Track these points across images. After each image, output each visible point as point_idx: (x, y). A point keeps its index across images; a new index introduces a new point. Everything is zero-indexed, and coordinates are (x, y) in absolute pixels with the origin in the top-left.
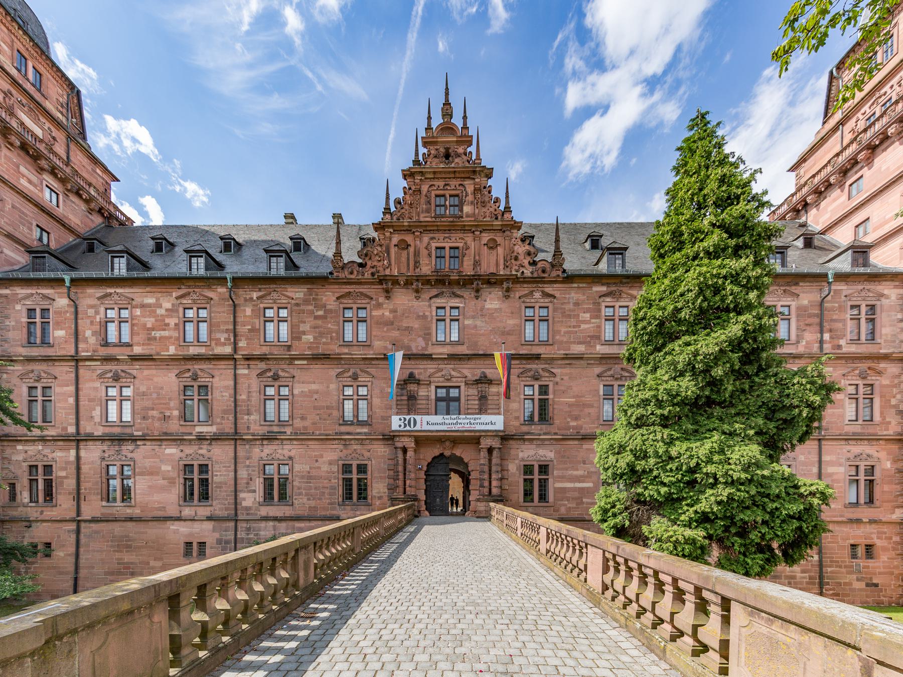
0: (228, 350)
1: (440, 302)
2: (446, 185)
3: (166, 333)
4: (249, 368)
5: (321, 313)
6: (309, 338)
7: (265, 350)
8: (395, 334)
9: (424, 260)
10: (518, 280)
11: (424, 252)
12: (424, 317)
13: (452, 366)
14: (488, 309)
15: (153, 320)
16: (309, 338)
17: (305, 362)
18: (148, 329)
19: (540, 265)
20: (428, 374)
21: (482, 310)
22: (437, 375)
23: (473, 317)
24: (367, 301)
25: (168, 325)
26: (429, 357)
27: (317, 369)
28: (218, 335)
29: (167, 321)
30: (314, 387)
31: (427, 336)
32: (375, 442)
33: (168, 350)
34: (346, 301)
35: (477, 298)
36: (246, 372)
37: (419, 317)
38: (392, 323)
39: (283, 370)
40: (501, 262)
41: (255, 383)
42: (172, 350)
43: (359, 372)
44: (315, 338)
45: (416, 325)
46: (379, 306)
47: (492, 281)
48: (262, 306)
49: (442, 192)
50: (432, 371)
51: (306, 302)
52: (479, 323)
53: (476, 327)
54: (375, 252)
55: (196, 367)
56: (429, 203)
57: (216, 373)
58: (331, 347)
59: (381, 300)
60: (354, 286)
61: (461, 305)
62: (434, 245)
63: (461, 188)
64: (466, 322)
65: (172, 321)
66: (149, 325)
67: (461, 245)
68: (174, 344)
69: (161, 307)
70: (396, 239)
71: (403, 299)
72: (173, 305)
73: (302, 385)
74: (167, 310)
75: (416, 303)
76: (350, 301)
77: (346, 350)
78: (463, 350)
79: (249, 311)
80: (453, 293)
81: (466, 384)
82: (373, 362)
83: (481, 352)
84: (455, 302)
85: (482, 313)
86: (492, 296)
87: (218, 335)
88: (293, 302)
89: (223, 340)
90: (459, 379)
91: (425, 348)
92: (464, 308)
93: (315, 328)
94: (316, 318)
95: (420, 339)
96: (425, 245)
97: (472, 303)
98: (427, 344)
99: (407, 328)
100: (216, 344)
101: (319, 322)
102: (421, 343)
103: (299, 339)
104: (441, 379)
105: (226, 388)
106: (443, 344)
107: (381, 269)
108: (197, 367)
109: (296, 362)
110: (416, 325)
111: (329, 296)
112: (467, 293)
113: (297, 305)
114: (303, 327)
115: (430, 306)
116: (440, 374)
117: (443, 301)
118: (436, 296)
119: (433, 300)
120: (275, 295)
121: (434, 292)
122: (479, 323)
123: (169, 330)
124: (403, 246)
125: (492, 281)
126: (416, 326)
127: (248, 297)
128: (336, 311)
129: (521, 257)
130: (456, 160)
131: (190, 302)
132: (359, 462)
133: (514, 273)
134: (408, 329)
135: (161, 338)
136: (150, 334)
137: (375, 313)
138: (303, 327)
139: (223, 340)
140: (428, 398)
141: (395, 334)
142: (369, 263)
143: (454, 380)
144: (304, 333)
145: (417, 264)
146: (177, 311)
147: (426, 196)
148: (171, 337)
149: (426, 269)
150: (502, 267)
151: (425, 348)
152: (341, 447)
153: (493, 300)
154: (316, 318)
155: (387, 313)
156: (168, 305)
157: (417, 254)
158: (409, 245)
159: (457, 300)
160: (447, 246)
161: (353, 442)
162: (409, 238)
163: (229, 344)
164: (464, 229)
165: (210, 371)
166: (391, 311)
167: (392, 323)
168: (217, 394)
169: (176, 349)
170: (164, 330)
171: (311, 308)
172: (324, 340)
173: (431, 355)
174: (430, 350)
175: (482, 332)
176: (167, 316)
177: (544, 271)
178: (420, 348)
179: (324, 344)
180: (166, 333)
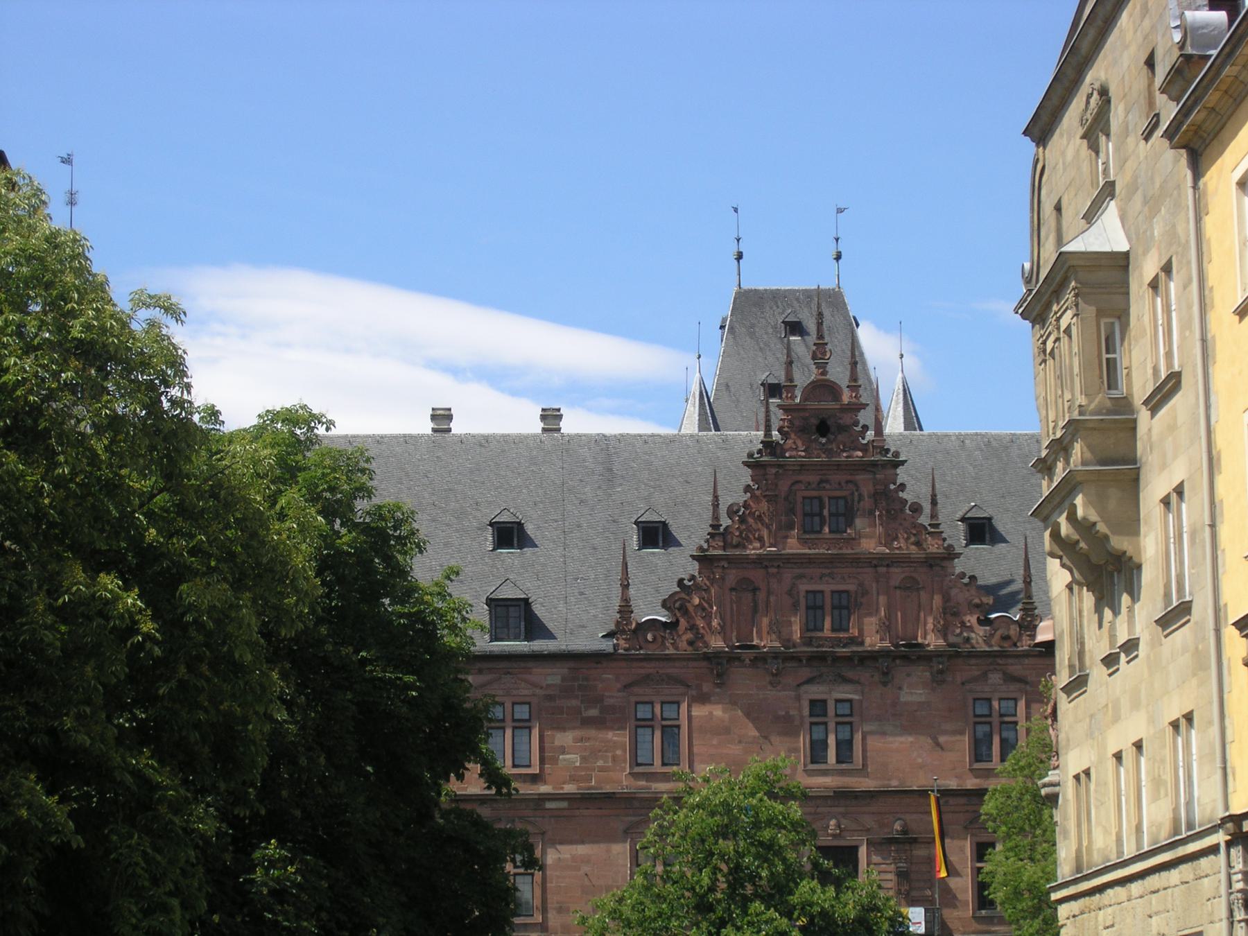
1: (816, 691)
2: (821, 481)
5: (593, 712)
6: (574, 758)
13: (842, 809)
16: (574, 758)
17: (564, 804)
44: (583, 759)
49: (815, 493)
54: (696, 601)
56: (792, 511)
59: (706, 687)
61: (856, 697)
62: (804, 587)
63: (850, 486)
81: (870, 843)
83: (894, 784)
92: (861, 701)
103: (555, 760)
109: (549, 805)
113: (550, 698)
117: (822, 688)
118: (810, 681)
121: (805, 673)
130: (840, 437)
144: (563, 750)
147: (786, 499)
158: (755, 590)
159: (849, 687)
172: (600, 763)
179: (602, 769)
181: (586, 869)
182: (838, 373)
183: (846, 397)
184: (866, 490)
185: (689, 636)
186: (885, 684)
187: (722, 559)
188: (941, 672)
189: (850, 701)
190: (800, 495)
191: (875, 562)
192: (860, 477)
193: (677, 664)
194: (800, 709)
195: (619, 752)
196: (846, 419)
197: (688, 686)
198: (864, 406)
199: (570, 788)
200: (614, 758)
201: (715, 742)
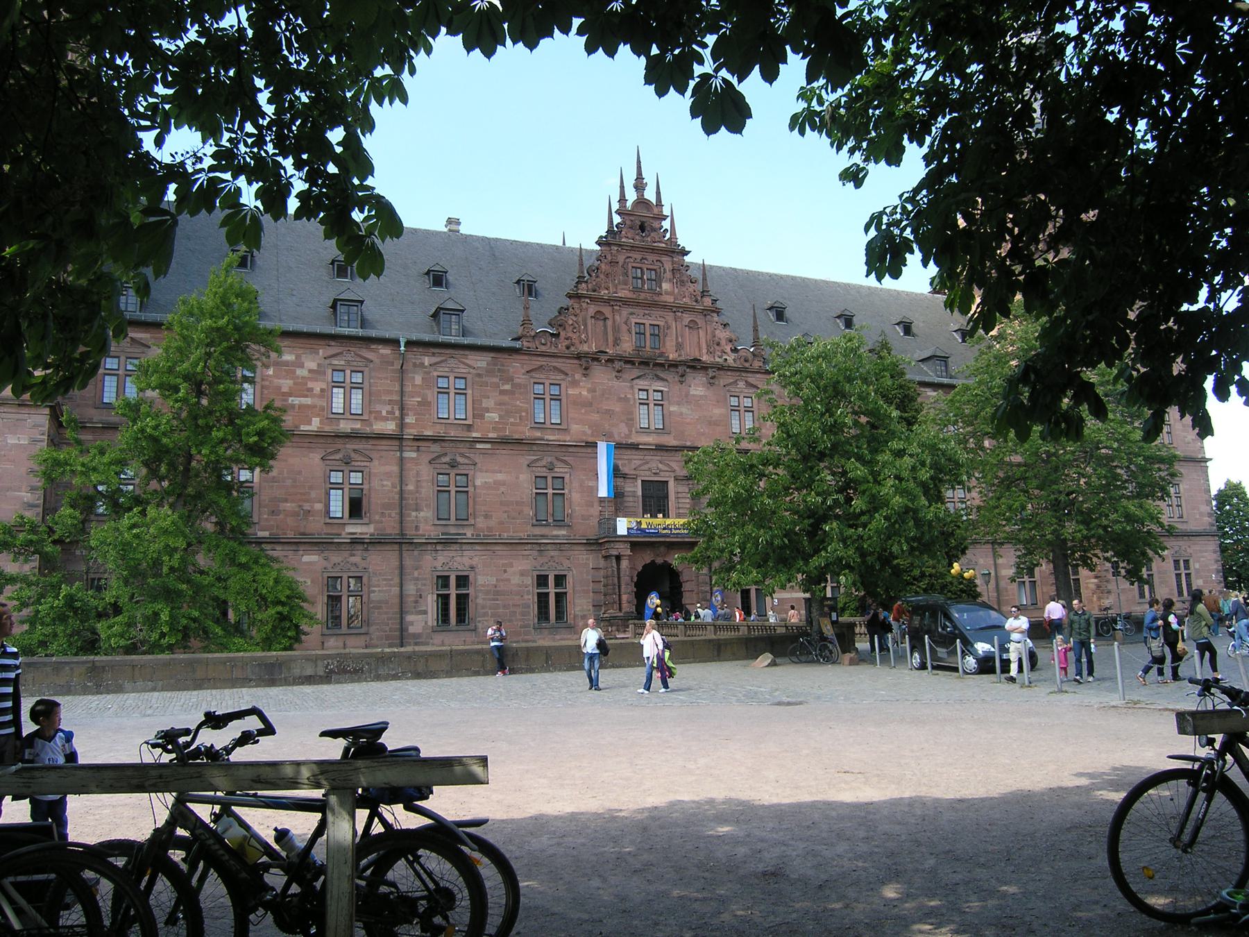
0: (390, 427)
1: (642, 383)
2: (643, 259)
3: (308, 401)
4: (418, 450)
5: (507, 387)
6: (494, 416)
7: (440, 431)
8: (595, 417)
9: (625, 337)
10: (721, 368)
11: (624, 328)
12: (626, 400)
14: (694, 395)
15: (290, 382)
16: (494, 416)
17: (488, 446)
18: (284, 394)
19: (741, 353)
20: (633, 467)
21: (687, 395)
22: (642, 468)
23: (679, 404)
24: (563, 377)
25: (311, 390)
26: (634, 447)
27: (504, 453)
28: (378, 407)
29: (310, 385)
30: (500, 477)
31: (630, 420)
32: (576, 547)
33: (310, 423)
34: (537, 376)
35: (681, 382)
36: (414, 455)
37: (620, 399)
38: (591, 404)
39: (462, 455)
40: (704, 346)
41: (426, 472)
42: (315, 425)
43: (556, 462)
44: (501, 417)
45: (617, 408)
46: (575, 384)
47: (695, 365)
48: (436, 374)
49: (639, 265)
50: (638, 462)
51: (490, 372)
52: (684, 410)
53: (681, 414)
55: (348, 446)
57: (374, 455)
58: (521, 428)
59: (577, 376)
60: (545, 359)
62: (634, 320)
63: (659, 263)
64: (672, 409)
65: (317, 387)
66: (285, 389)
67: (661, 324)
68: (318, 415)
69: (302, 366)
70: (592, 309)
71: (602, 376)
72: (319, 365)
73: (484, 474)
74: (310, 371)
75: (616, 383)
76: (542, 376)
77: (538, 434)
78: (671, 441)
79: (418, 380)
80: (657, 376)
81: (676, 479)
82: (571, 449)
84: (659, 385)
85: (686, 399)
86: (696, 381)
87: (378, 407)
88: (474, 371)
89: (384, 413)
90: (667, 474)
91: (628, 436)
93: (500, 404)
94: (503, 392)
95: (623, 425)
96: (624, 320)
97: (678, 387)
98: (630, 431)
99: (607, 411)
100: (376, 418)
101: (506, 398)
102: (623, 429)
103: (482, 417)
104: (648, 473)
105: (388, 475)
106: (646, 431)
107: (577, 342)
108: (351, 446)
109: (479, 446)
110: (617, 408)
111: (517, 367)
112: (671, 376)
113: (479, 375)
114: (488, 403)
115: (632, 387)
116: (646, 467)
118: (638, 377)
119: (637, 381)
120: (452, 362)
121: (636, 372)
122: (684, 410)
123: (313, 396)
124: (599, 316)
125: (695, 365)
126: (617, 409)
127: (418, 362)
128: (525, 386)
129: (723, 342)
130: (652, 234)
131: (343, 363)
132: (557, 573)
133: (717, 359)
134: (609, 413)
135: (300, 406)
136: (287, 400)
137: (571, 391)
138: (488, 403)
139: (384, 413)
140: (634, 494)
141: (595, 417)
142: (563, 334)
143: (662, 474)
144: (487, 410)
145: (617, 342)
146: (325, 373)
147: (622, 266)
148: (315, 406)
149: (627, 346)
150: (704, 351)
151: (628, 436)
152: (536, 553)
153: (697, 387)
154: (503, 392)
155: (585, 393)
156: (313, 365)
157: (616, 329)
158: (605, 319)
159: (661, 383)
160: (647, 322)
161: (549, 547)
162: (607, 310)
163: (393, 419)
164: (665, 307)
165: (367, 452)
166: (589, 391)
167: (591, 404)
168: (376, 483)
169: (321, 422)
170: (306, 396)
171: (496, 380)
172: (512, 420)
173: (638, 445)
174: (635, 439)
175: (688, 420)
176: (311, 379)
177: (746, 361)
178: (623, 435)
179: (512, 424)
180: (308, 401)
181: (502, 489)
182: (650, 195)
183: (656, 211)
184: (668, 266)
185: (567, 343)
186: (681, 382)
187: (586, 297)
188: (713, 378)
189: (661, 391)
190: (630, 265)
191: (674, 309)
192: (664, 259)
193: (559, 360)
194: (633, 394)
195: (524, 414)
196: (656, 224)
197: (567, 374)
198: (665, 218)
199: (491, 435)
200: (521, 418)
201: (583, 411)
